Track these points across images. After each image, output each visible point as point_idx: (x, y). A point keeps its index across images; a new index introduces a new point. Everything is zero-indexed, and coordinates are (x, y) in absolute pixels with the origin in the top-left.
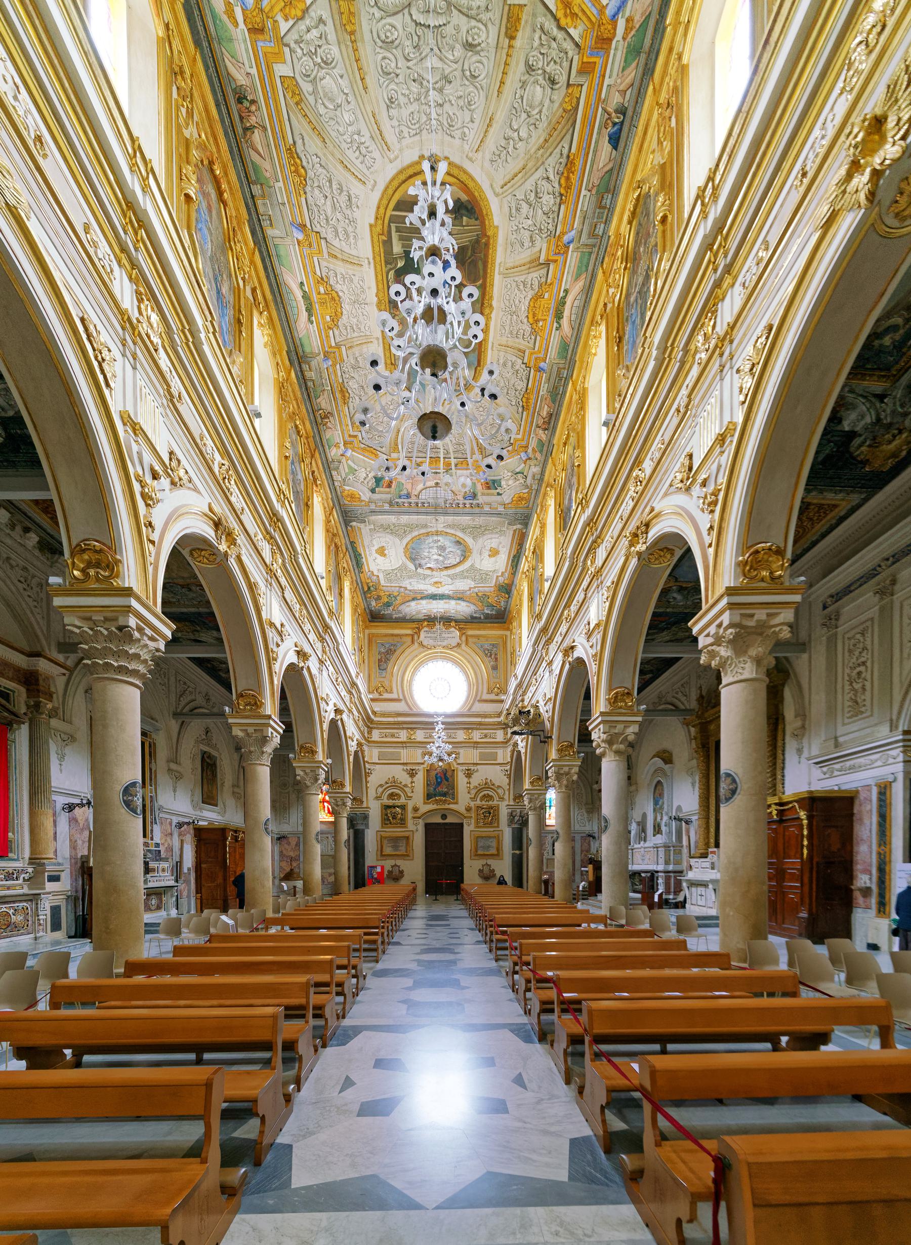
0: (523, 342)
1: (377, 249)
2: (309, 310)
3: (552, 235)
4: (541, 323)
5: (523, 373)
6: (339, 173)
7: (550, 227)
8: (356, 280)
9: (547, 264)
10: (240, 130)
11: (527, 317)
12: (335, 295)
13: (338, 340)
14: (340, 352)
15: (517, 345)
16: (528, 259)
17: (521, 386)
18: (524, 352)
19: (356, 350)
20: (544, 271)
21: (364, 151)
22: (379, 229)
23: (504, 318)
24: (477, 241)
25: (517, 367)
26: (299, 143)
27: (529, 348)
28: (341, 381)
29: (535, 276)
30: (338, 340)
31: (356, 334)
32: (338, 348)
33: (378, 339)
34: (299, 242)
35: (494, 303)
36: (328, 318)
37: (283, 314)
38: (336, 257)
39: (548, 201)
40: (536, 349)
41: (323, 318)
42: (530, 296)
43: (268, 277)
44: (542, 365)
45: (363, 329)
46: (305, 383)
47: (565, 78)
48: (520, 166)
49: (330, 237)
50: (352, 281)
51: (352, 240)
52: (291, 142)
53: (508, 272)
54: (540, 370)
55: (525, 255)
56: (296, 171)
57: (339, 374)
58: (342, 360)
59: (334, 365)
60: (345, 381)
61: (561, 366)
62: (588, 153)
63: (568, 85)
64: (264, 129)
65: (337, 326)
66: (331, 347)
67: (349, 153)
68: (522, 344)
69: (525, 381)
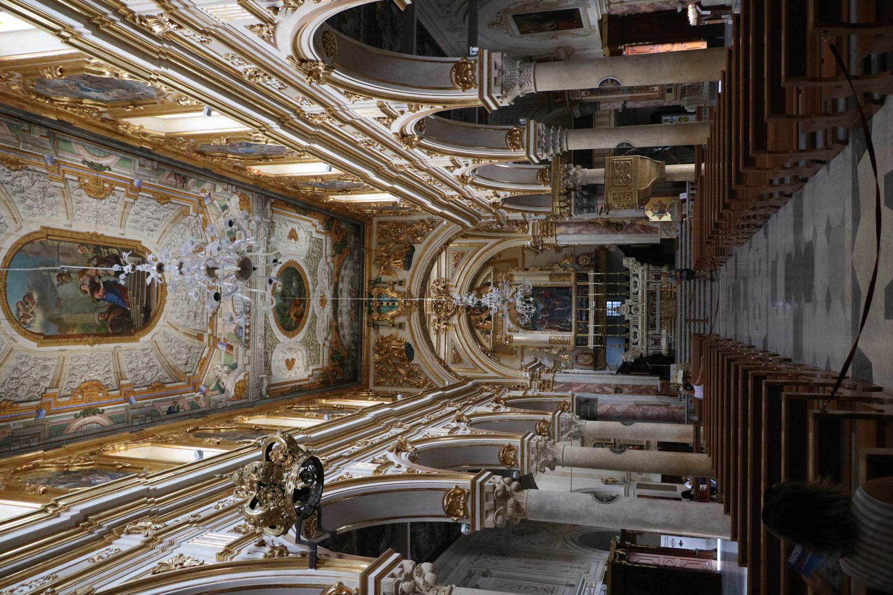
0: (65, 383)
1: (130, 243)
2: (91, 165)
3: (133, 385)
4: (80, 397)
5: (36, 392)
6: (161, 228)
7: (138, 382)
8: (112, 219)
9: (120, 387)
10: (176, 171)
11: (86, 381)
12: (103, 196)
13: (70, 183)
14: (57, 180)
15: (62, 378)
16: (122, 371)
17: (22, 394)
18: (57, 387)
19: (59, 199)
20: (116, 387)
21: (169, 247)
22: (140, 248)
23: (85, 358)
24: (133, 326)
25: (42, 384)
26: (172, 206)
27: (60, 392)
28: (30, 167)
29: (112, 380)
30: (70, 183)
31: (75, 204)
32: (63, 180)
33: (71, 226)
34: (132, 181)
35: (96, 346)
36: (87, 181)
37: (91, 138)
38: (125, 207)
39: (149, 376)
40: (59, 400)
41: (88, 176)
42: (100, 379)
43: (118, 142)
44: (44, 412)
45: (78, 213)
46: (30, 122)
47: (188, 370)
48: (163, 353)
49: (136, 208)
50: (112, 215)
51: (134, 224)
52: (173, 201)
53: (115, 354)
54: (39, 410)
55: (125, 368)
56: (162, 198)
57: (37, 169)
58: (51, 179)
59: (46, 167)
60: (30, 173)
61: (42, 436)
62: (166, 396)
63: (186, 373)
64: (176, 187)
65: (80, 188)
66: (64, 172)
67: (168, 238)
68: (63, 384)
69: (27, 398)
